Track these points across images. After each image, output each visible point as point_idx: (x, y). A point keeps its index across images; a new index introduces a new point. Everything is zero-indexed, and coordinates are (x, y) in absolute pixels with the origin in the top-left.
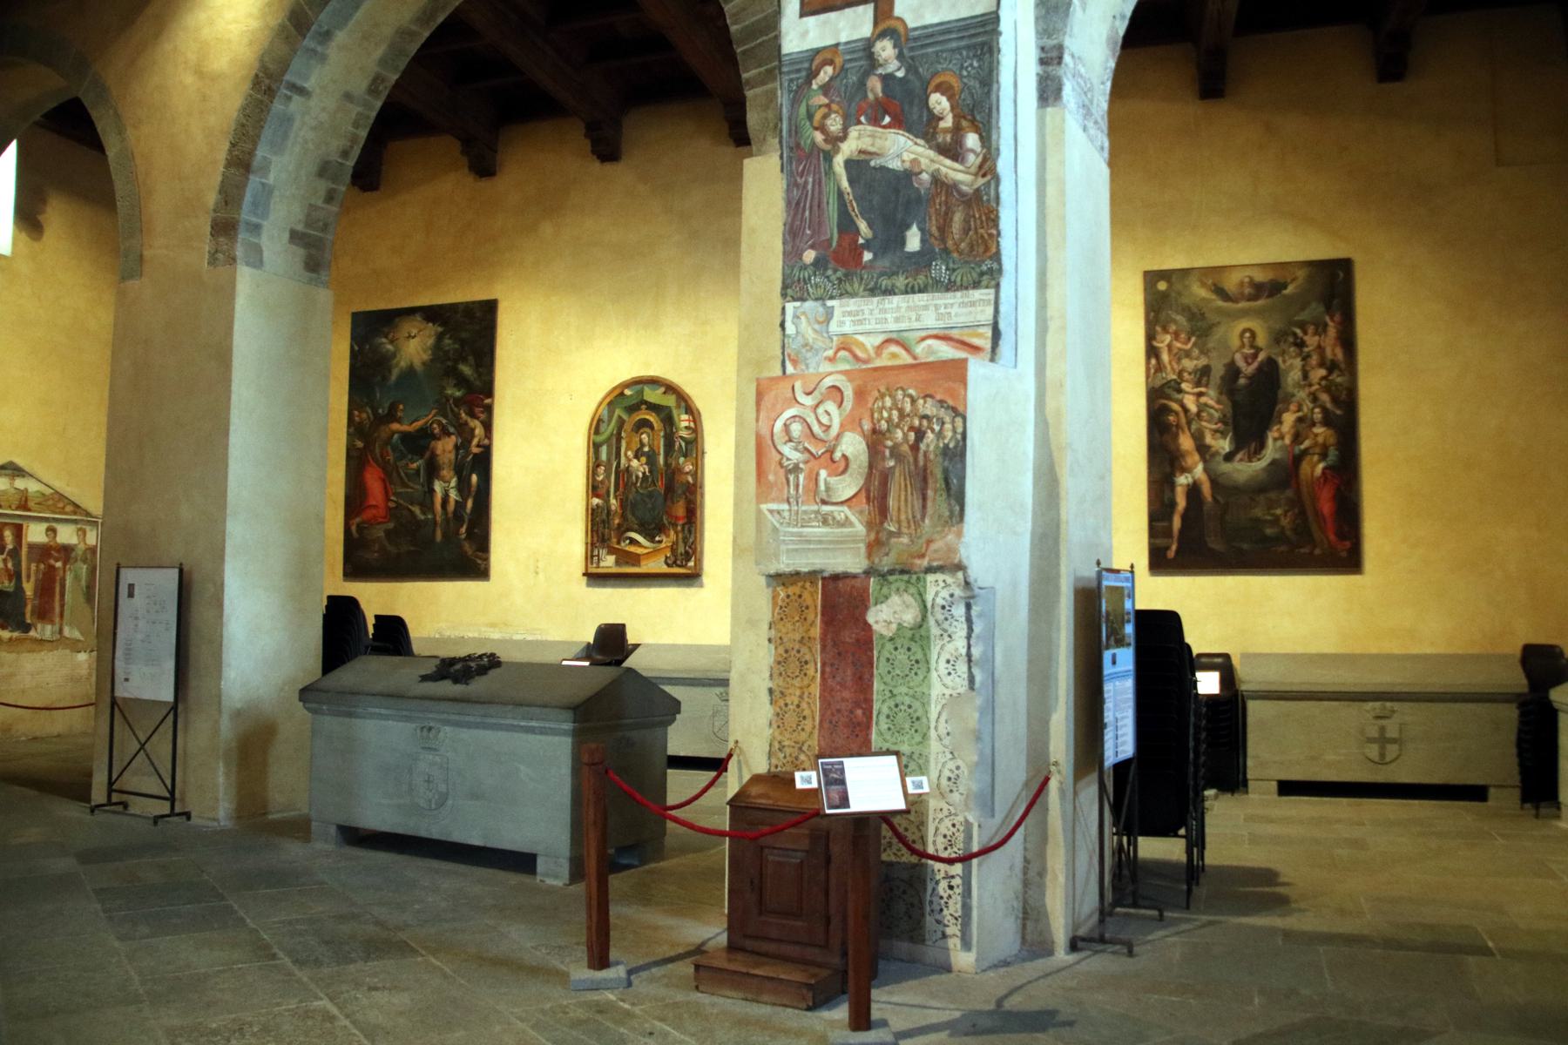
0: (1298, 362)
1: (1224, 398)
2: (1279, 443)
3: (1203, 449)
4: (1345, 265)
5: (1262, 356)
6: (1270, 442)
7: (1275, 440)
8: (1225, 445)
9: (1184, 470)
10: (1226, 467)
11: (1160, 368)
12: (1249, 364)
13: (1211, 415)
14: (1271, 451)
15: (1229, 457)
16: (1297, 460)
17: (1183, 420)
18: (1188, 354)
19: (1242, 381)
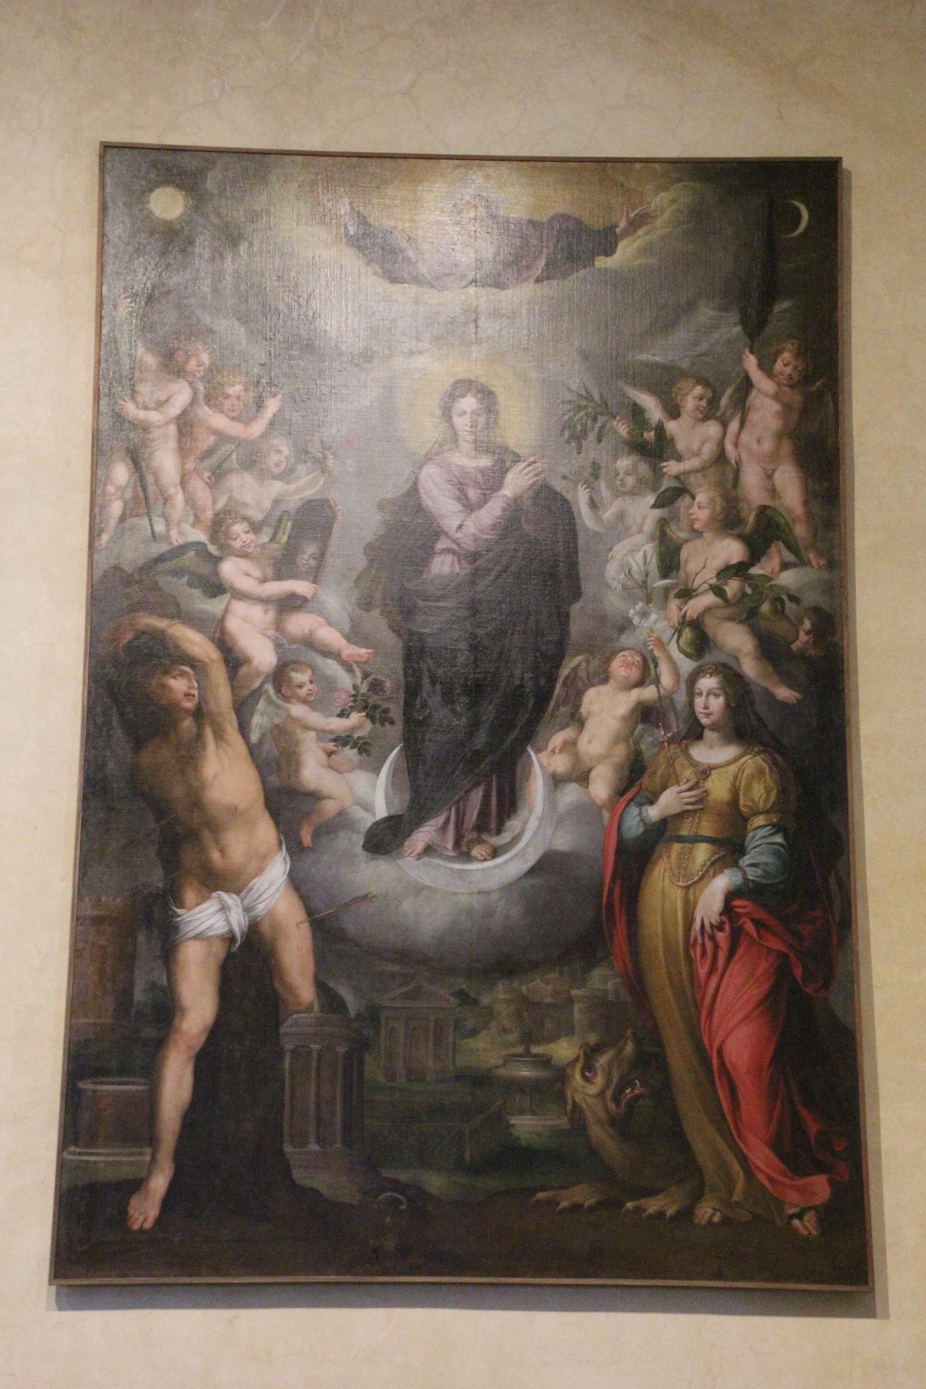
0: (643, 511)
1: (376, 622)
2: (571, 794)
3: (288, 804)
4: (817, 183)
5: (516, 482)
6: (537, 789)
7: (556, 781)
8: (370, 792)
9: (215, 880)
10: (373, 875)
11: (144, 497)
12: (470, 508)
13: (327, 684)
14: (546, 819)
15: (385, 839)
16: (635, 858)
17: (222, 697)
18: (252, 460)
19: (443, 566)
